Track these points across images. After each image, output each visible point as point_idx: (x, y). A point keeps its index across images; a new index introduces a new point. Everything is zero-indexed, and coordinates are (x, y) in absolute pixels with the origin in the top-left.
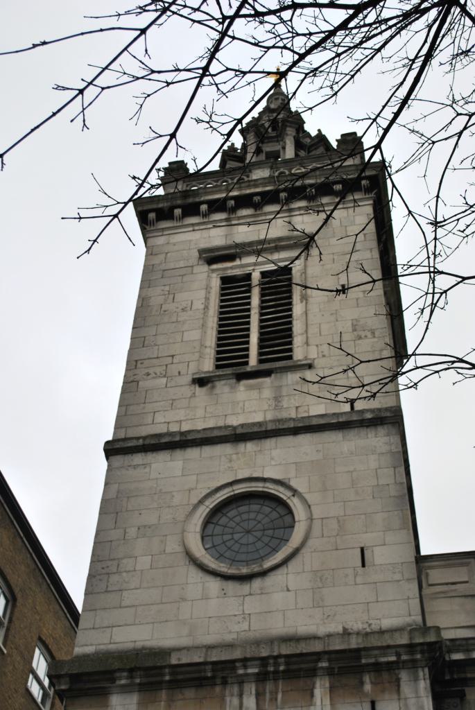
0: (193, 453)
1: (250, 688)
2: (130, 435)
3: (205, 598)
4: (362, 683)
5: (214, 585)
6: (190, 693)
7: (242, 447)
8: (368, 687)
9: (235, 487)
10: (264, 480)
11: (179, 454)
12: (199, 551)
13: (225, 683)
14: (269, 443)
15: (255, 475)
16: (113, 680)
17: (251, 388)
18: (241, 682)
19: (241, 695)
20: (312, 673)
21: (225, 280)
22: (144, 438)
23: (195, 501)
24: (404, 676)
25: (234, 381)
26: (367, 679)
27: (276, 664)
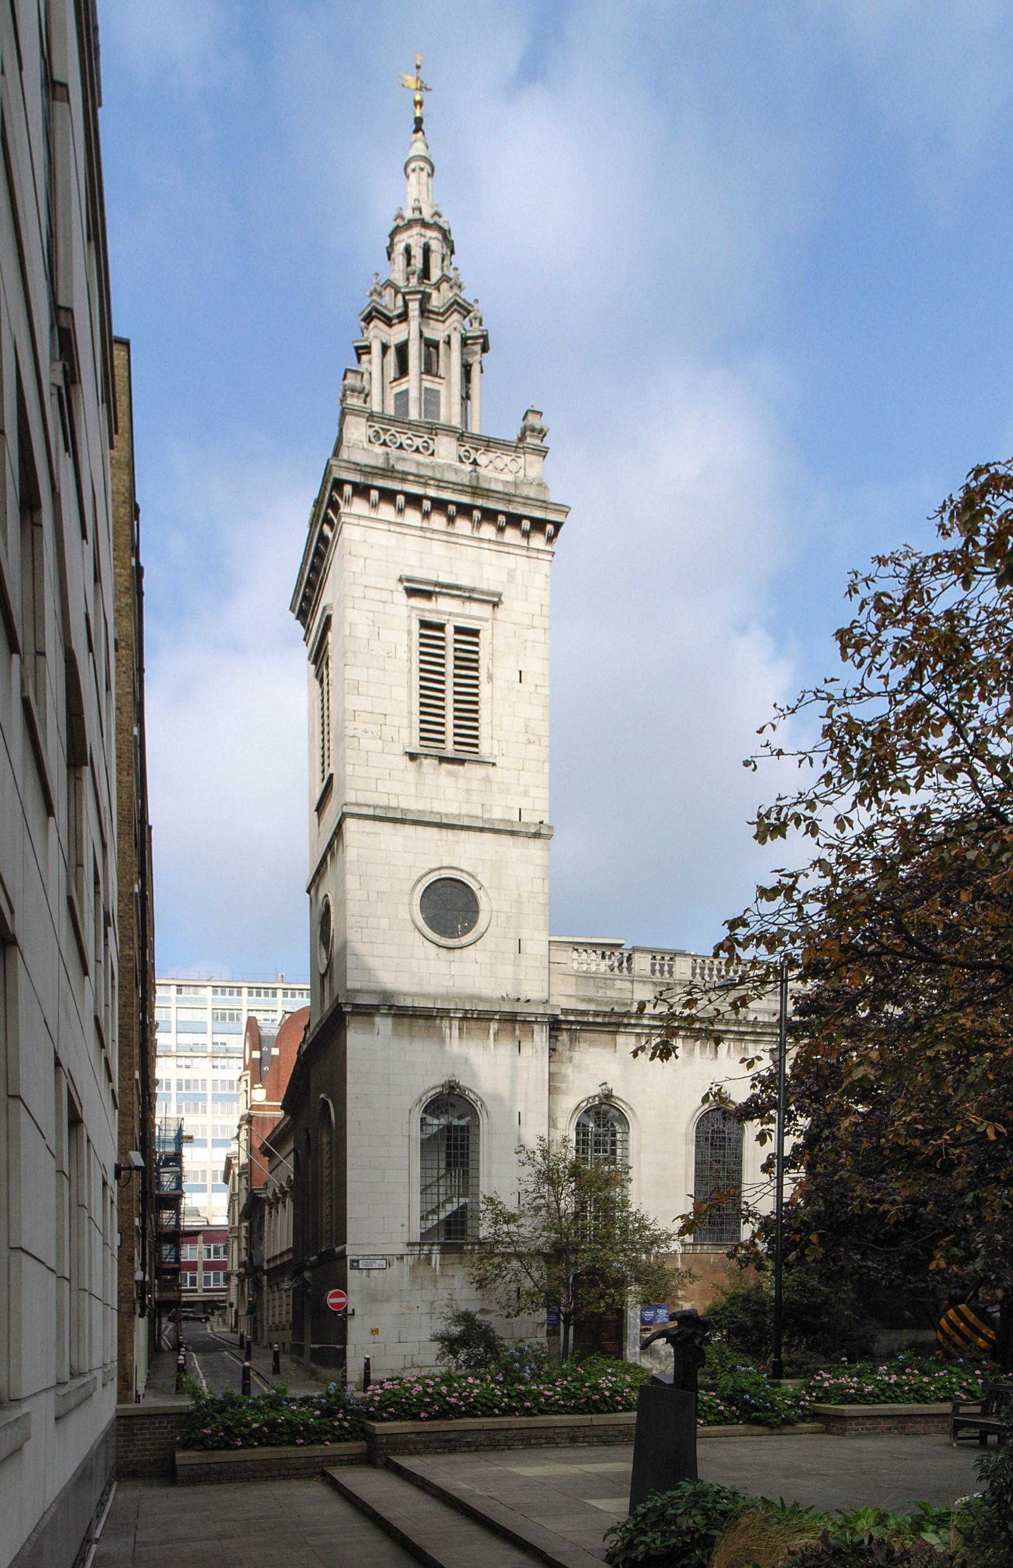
0: (410, 829)
1: (456, 1024)
2: (361, 801)
3: (427, 959)
4: (514, 1030)
5: (432, 948)
6: (422, 1022)
7: (444, 831)
8: (517, 1032)
9: (442, 871)
10: (462, 871)
11: (399, 826)
12: (421, 923)
13: (442, 1018)
14: (463, 835)
15: (454, 865)
16: (378, 1010)
17: (450, 774)
18: (451, 1019)
19: (450, 1028)
20: (491, 1020)
21: (424, 624)
22: (375, 807)
23: (416, 878)
24: (536, 1027)
25: (437, 762)
26: (517, 1027)
27: (472, 1014)
